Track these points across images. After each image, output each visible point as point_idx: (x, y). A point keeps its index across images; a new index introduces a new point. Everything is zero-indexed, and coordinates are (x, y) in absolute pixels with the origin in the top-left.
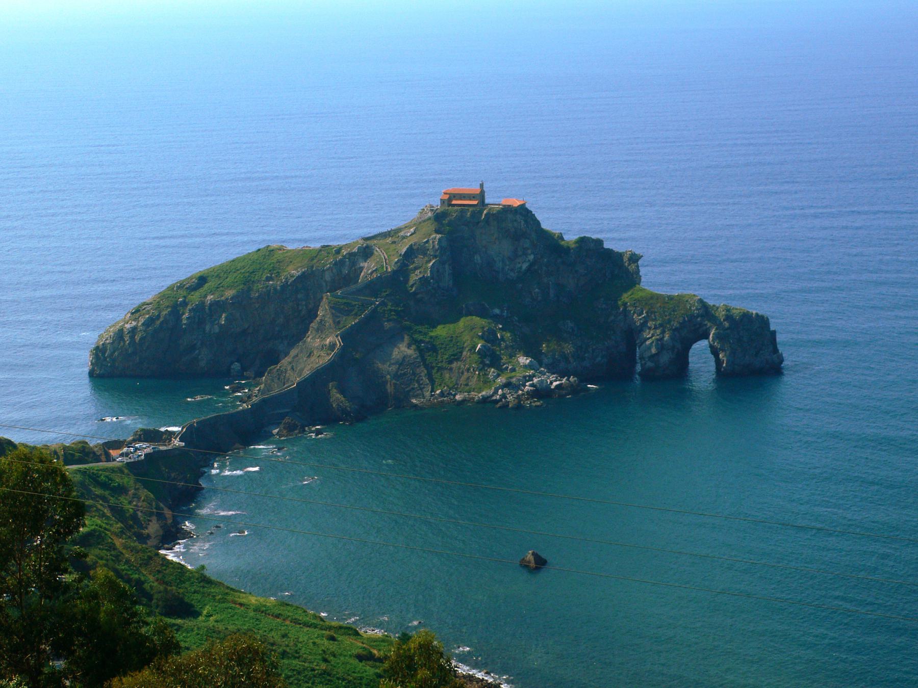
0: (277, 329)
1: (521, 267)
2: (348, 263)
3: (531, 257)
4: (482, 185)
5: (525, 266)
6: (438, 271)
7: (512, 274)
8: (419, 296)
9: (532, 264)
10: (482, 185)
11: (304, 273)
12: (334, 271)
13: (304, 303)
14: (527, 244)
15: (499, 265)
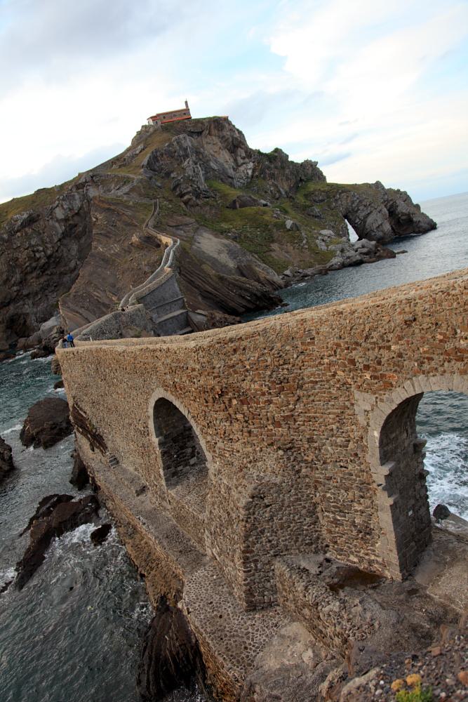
0: (15, 288)
1: (248, 173)
2: (77, 197)
3: (251, 165)
4: (186, 103)
5: (250, 172)
6: (194, 171)
7: (242, 181)
8: (186, 197)
9: (254, 171)
10: (186, 103)
11: (30, 215)
12: (65, 207)
13: (41, 249)
14: (244, 155)
15: (231, 172)
